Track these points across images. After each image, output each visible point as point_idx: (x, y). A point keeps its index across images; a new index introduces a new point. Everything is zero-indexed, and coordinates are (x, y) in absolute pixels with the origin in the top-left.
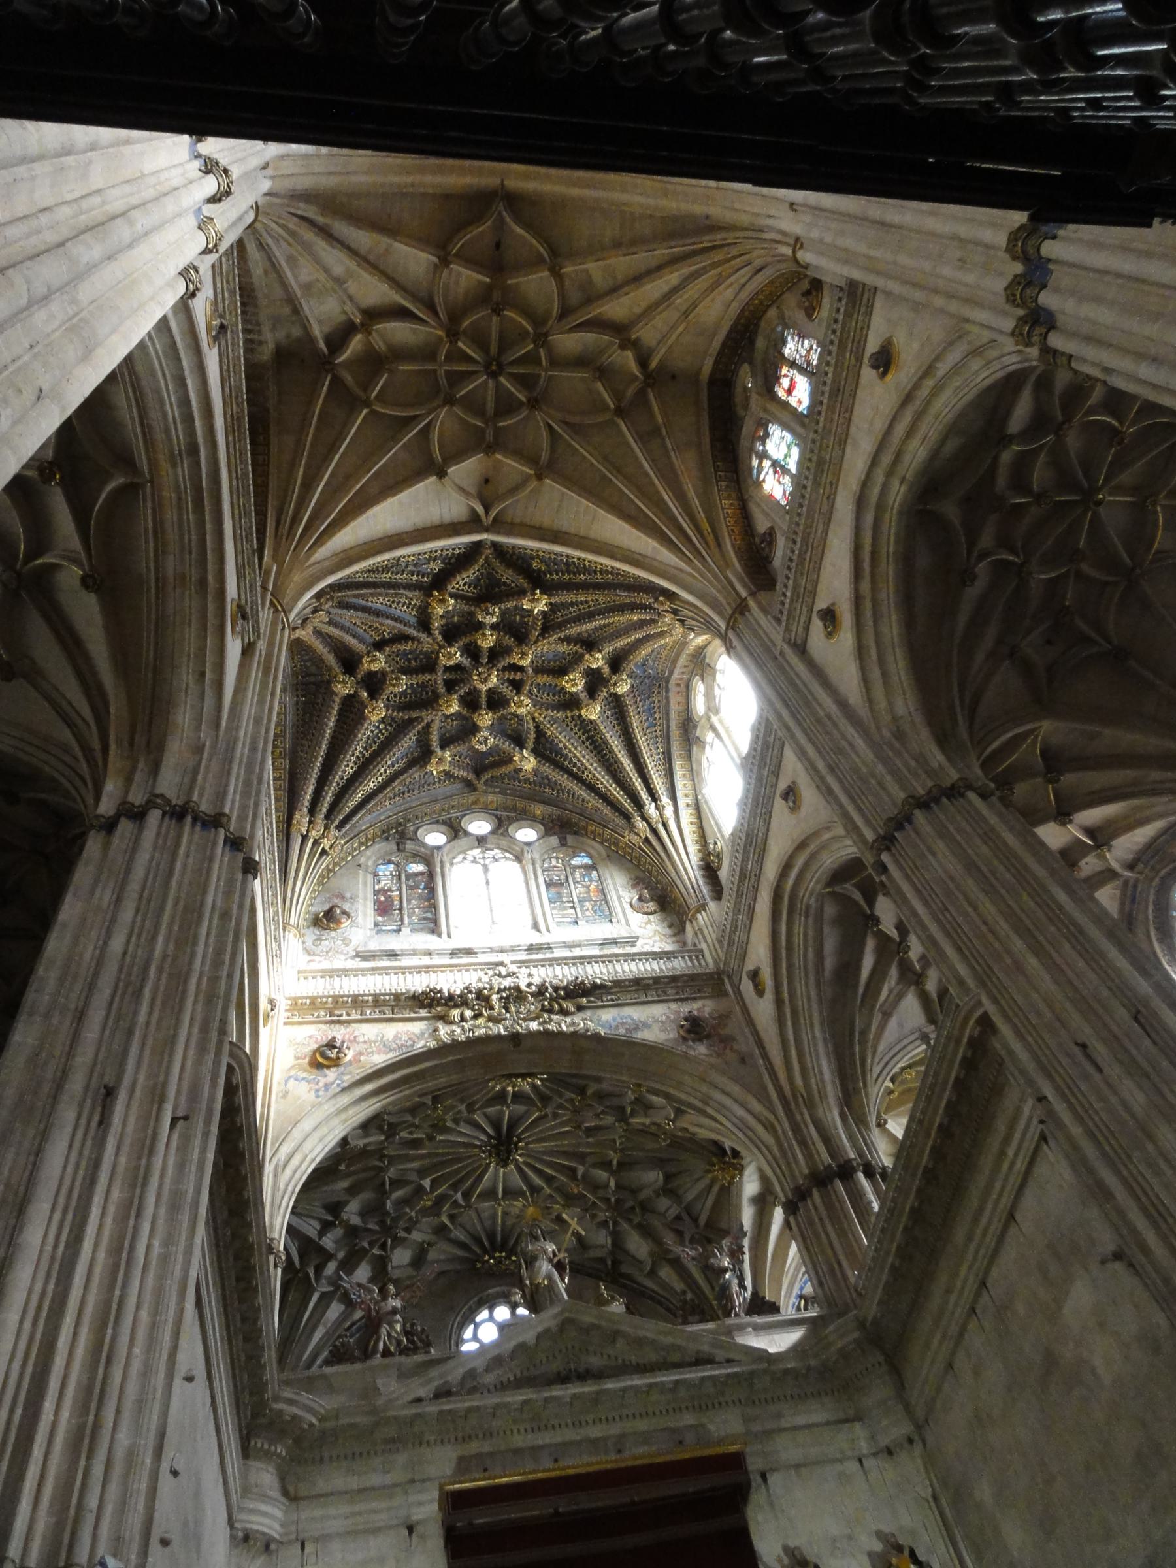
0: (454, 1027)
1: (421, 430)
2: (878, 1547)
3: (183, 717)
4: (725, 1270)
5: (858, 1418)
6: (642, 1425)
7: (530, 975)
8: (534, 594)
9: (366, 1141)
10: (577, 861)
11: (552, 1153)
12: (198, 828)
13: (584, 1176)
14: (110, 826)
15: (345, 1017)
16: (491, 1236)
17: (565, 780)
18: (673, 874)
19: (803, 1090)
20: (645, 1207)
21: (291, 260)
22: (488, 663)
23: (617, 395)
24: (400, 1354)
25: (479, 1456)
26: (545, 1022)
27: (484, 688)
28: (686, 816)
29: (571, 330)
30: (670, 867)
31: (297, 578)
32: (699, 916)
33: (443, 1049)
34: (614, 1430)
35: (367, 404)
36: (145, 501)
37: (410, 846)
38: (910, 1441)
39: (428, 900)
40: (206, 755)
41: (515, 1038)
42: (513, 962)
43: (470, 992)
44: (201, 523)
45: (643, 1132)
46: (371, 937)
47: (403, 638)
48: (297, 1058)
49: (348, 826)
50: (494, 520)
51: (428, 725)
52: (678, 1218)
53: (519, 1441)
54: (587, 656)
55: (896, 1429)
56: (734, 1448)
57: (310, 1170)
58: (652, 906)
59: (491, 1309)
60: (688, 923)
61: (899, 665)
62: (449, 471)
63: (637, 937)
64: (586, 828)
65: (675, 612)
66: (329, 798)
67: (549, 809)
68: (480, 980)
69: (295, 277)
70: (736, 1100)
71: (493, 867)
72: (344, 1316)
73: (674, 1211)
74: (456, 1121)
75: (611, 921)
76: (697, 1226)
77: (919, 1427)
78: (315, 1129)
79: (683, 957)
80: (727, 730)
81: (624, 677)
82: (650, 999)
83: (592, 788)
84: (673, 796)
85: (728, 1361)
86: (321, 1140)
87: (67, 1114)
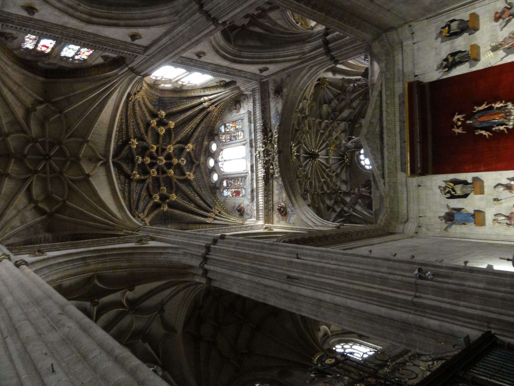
0: (275, 172)
1: (73, 183)
2: (440, 39)
3: (175, 258)
4: (354, 85)
5: (402, 43)
6: (397, 114)
7: (259, 147)
8: (130, 144)
9: (309, 199)
10: (223, 131)
11: (316, 141)
12: (210, 253)
13: (323, 130)
14: (210, 280)
15: (271, 206)
16: (340, 160)
17: (197, 134)
18: (227, 97)
19: (299, 56)
20: (334, 110)
21: (12, 228)
22: (155, 159)
24: (371, 189)
25: (401, 165)
27: (164, 161)
28: (207, 93)
29: (30, 129)
31: (128, 223)
32: (241, 89)
33: (282, 176)
34: (398, 123)
35: (64, 201)
36: (104, 273)
37: (218, 185)
38: (410, 26)
39: (235, 179)
40: (187, 251)
41: (279, 152)
42: (255, 153)
43: (265, 166)
44: (109, 255)
45: (311, 110)
46: (247, 198)
47: (148, 189)
48: (283, 220)
49: (211, 205)
50: (104, 157)
51: (178, 180)
52: (338, 100)
53: (398, 153)
54: (152, 125)
55: (406, 31)
56: (406, 86)
57: (317, 216)
58: (238, 106)
59: (361, 160)
60: (244, 93)
61: (150, 11)
62: (87, 173)
63: (248, 111)
65: (135, 94)
66: (202, 212)
68: (260, 163)
69: (19, 226)
70: (302, 79)
71: (225, 158)
72: (360, 205)
73: (336, 102)
74: (305, 171)
75: (243, 119)
77: (406, 23)
78: (305, 215)
79: (255, 95)
80: (177, 77)
81: (159, 113)
83: (198, 125)
84: (201, 97)
85: (381, 86)
86: (308, 213)
87: (294, 289)
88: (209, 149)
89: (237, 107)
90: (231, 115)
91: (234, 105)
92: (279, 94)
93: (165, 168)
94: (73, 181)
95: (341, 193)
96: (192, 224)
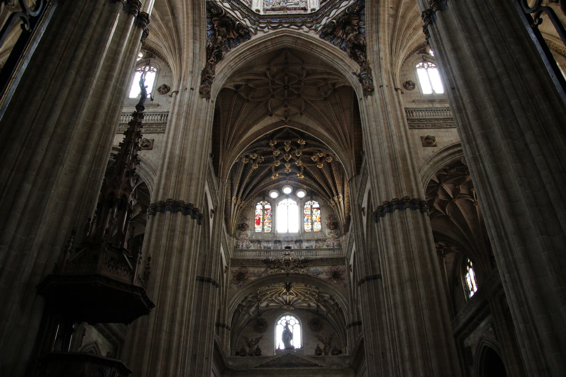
8: (301, 140)
12: (206, 283)
13: (310, 293)
15: (245, 265)
19: (356, 299)
23: (326, 94)
26: (295, 270)
30: (339, 217)
35: (248, 101)
37: (266, 198)
39: (270, 220)
41: (288, 274)
48: (233, 277)
50: (289, 120)
51: (271, 167)
64: (319, 195)
66: (242, 191)
67: (308, 187)
73: (332, 303)
76: (338, 307)
82: (325, 264)
88: (301, 188)
89: (331, 226)
90: (326, 218)
91: (334, 221)
92: (333, 276)
93: (281, 158)
94: (267, 103)
95: (258, 304)
96: (231, 182)
